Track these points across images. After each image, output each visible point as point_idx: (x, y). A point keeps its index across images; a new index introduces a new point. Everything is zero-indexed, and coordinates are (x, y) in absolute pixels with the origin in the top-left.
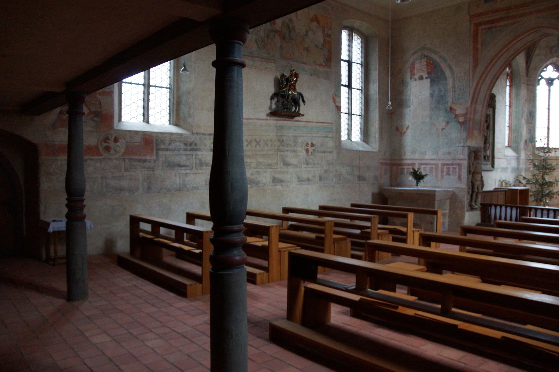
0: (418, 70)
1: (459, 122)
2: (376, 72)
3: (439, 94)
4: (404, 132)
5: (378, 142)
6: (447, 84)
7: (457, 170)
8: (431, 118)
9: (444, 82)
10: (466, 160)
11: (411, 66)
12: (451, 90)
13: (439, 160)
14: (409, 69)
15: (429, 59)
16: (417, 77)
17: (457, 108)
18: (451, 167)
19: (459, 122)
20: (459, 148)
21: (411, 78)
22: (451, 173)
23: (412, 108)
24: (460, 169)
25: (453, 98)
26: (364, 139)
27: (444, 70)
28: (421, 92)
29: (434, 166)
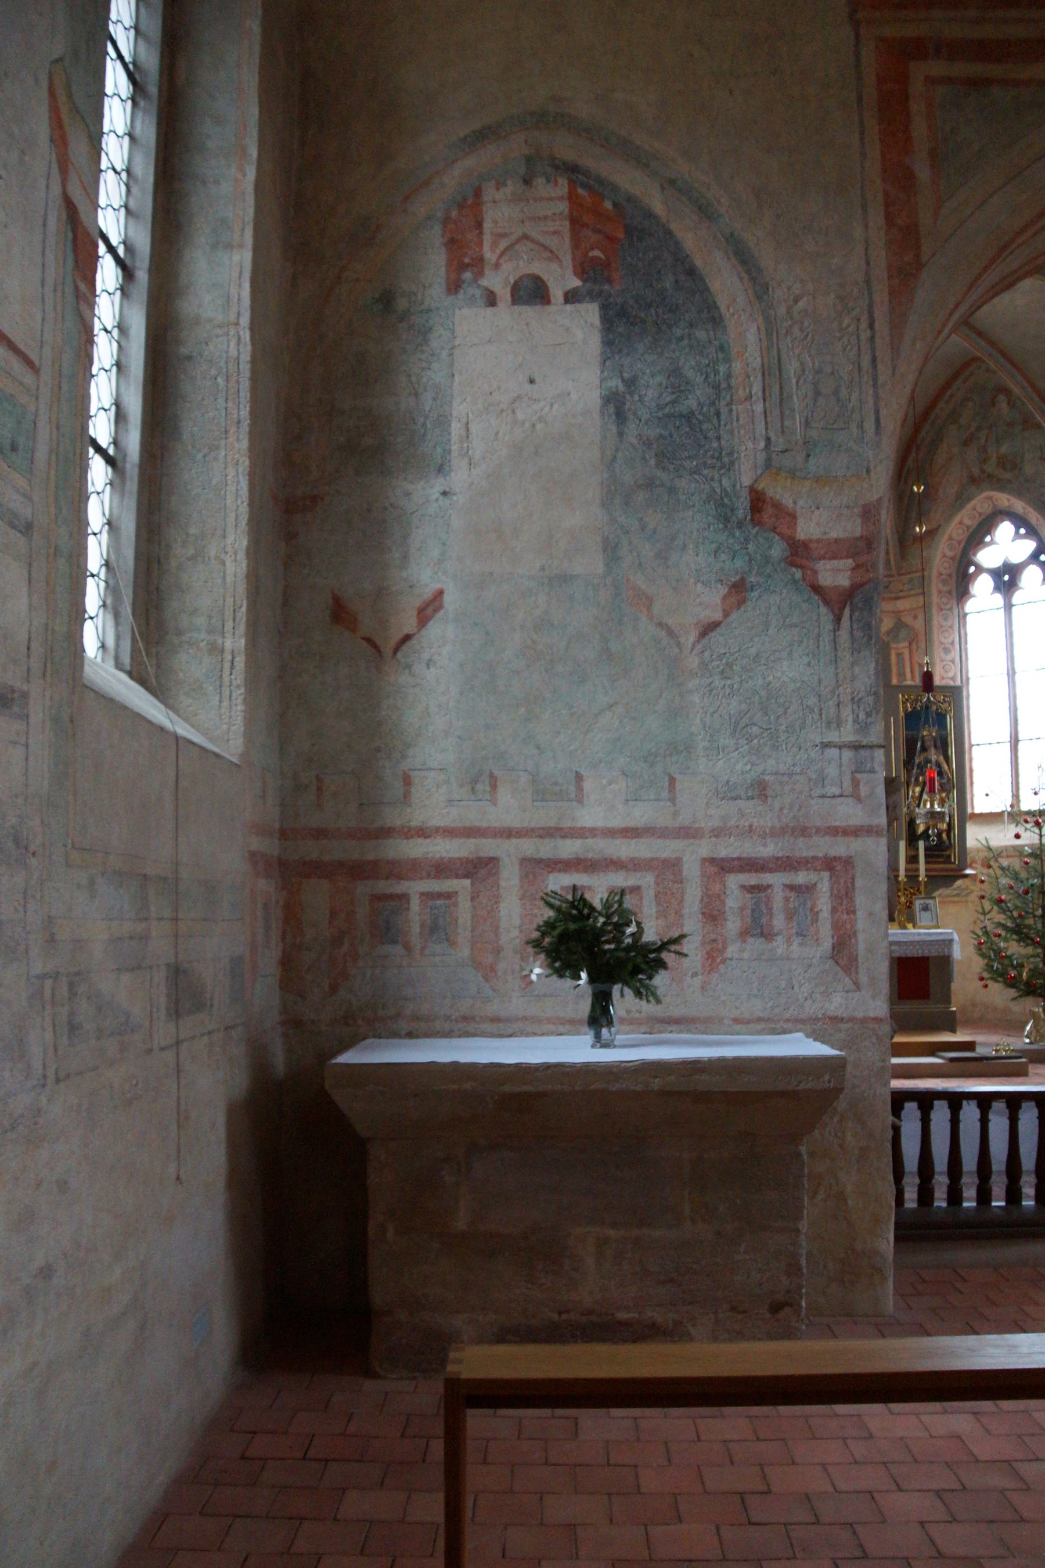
0: (503, 244)
1: (816, 589)
2: (241, 170)
3: (673, 402)
4: (399, 636)
5: (239, 694)
6: (721, 348)
7: (824, 903)
8: (611, 551)
9: (701, 334)
10: (869, 831)
11: (454, 213)
12: (757, 389)
13: (687, 833)
14: (437, 229)
15: (584, 186)
16: (497, 281)
17: (801, 503)
18: (776, 880)
19: (816, 589)
20: (834, 752)
21: (454, 287)
22: (779, 921)
23: (460, 477)
24: (844, 898)
25: (768, 440)
26: (135, 652)
27: (698, 263)
28: (532, 381)
29: (647, 880)
